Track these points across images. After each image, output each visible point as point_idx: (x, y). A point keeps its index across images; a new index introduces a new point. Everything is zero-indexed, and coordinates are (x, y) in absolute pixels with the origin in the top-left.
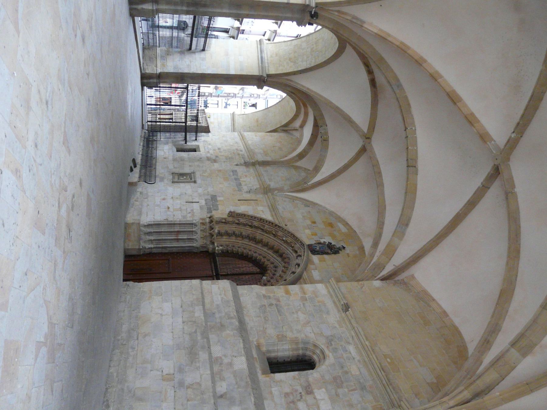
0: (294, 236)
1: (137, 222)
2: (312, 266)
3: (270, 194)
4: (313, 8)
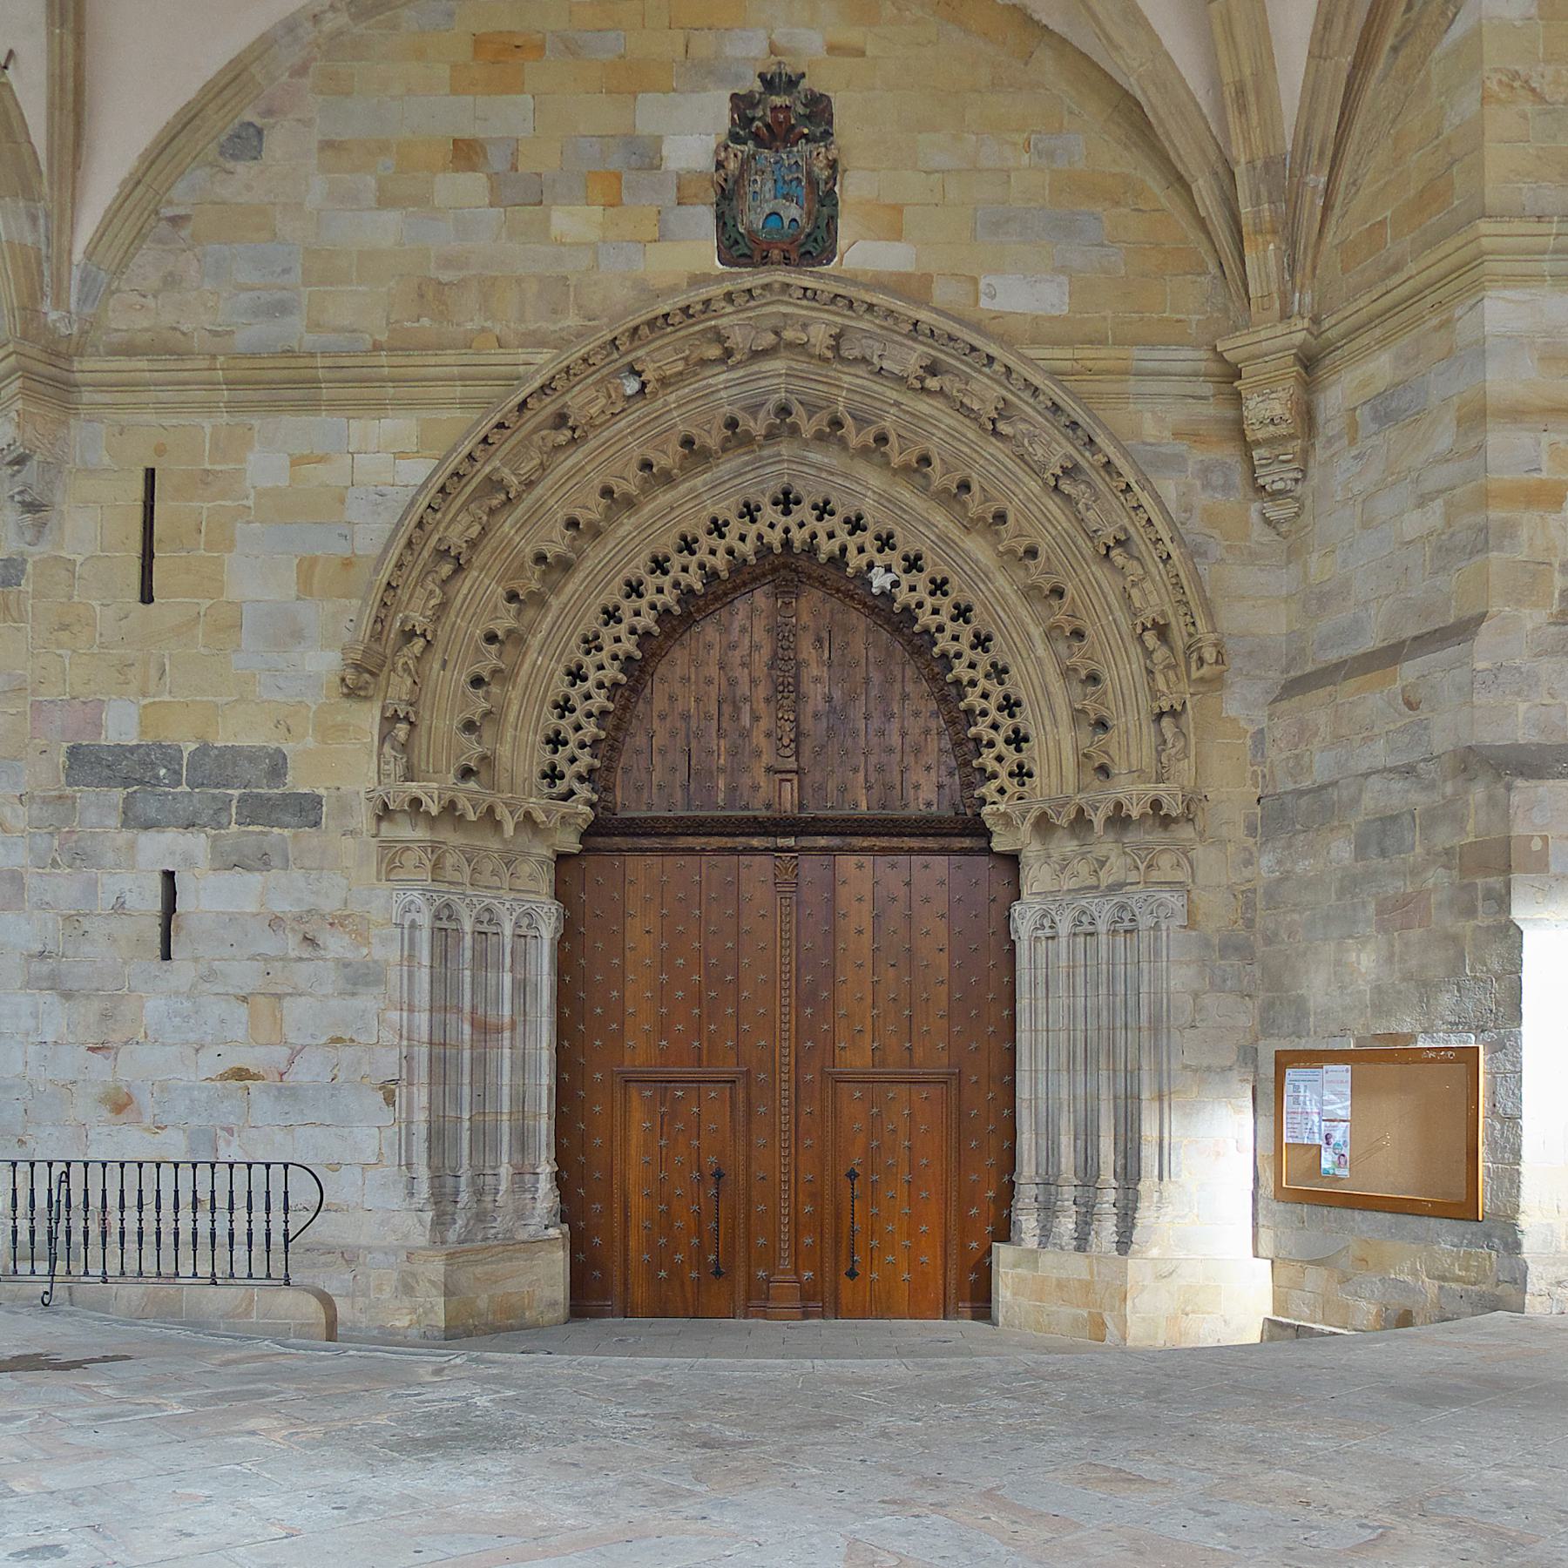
2: (943, 293)
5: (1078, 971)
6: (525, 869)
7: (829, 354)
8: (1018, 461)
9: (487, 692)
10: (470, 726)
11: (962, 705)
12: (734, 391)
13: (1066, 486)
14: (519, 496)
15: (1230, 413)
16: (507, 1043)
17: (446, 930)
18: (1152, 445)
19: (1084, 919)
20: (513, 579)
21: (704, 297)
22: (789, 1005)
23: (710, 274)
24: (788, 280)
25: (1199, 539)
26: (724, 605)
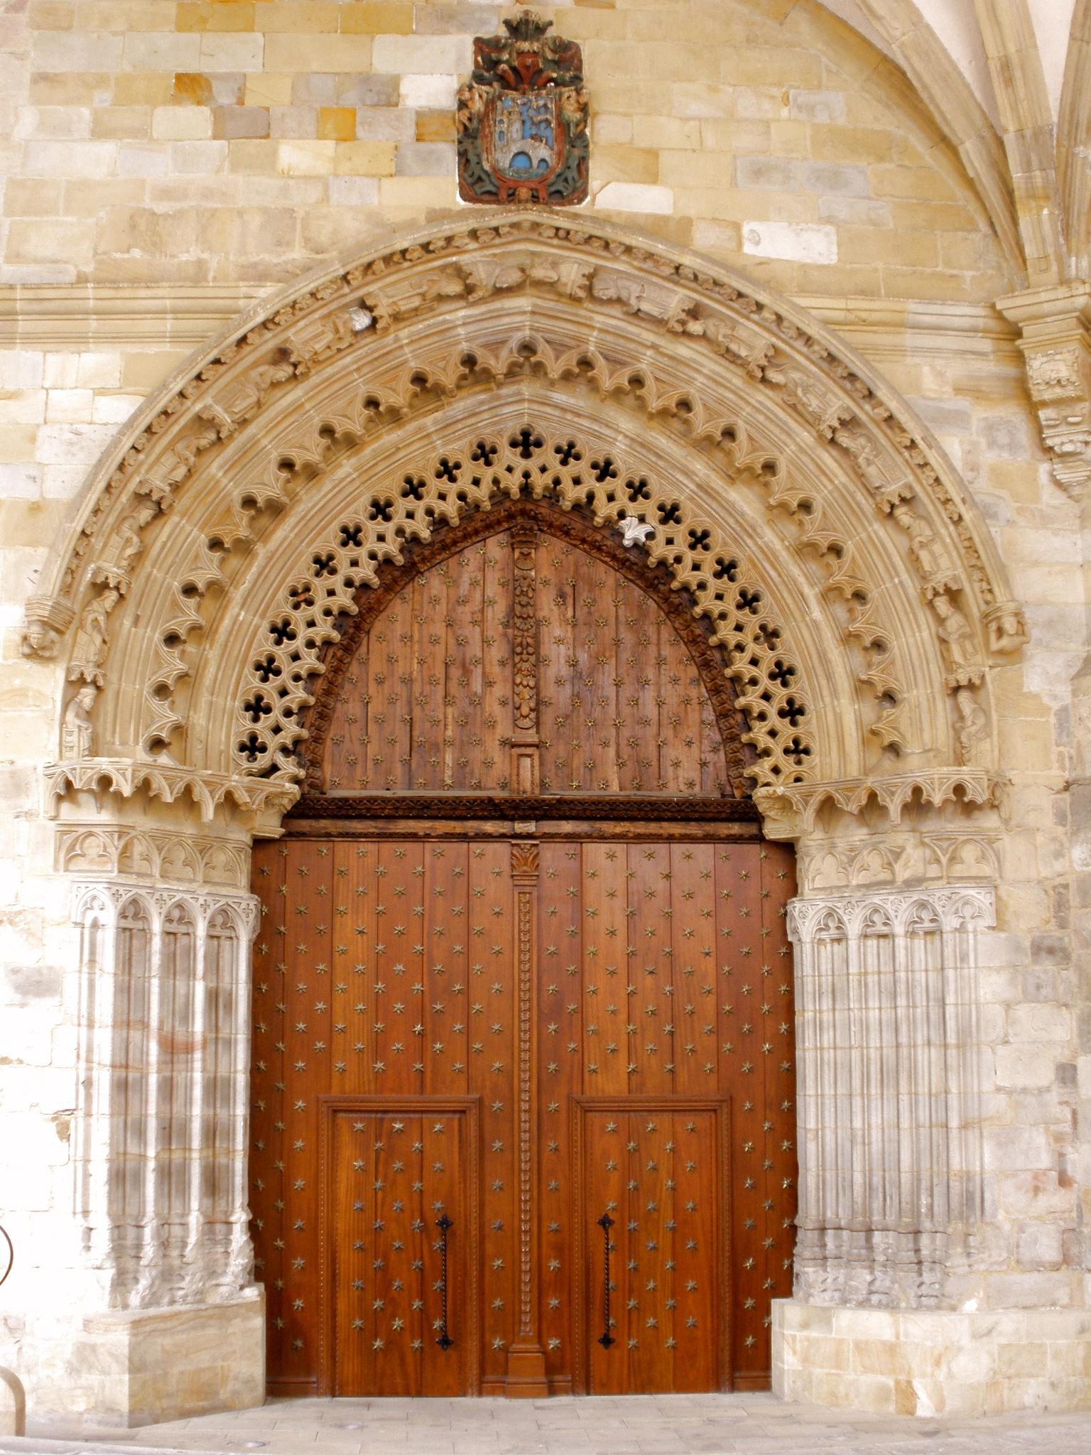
2: (705, 237)
5: (870, 978)
6: (220, 858)
7: (581, 294)
8: (789, 410)
9: (183, 652)
10: (161, 690)
11: (728, 672)
12: (471, 328)
13: (844, 438)
14: (230, 436)
15: (1010, 370)
16: (198, 1065)
17: (131, 930)
18: (930, 399)
19: (876, 918)
20: (218, 525)
21: (448, 233)
22: (529, 1020)
23: (450, 210)
24: (538, 220)
25: (988, 500)
26: (452, 555)
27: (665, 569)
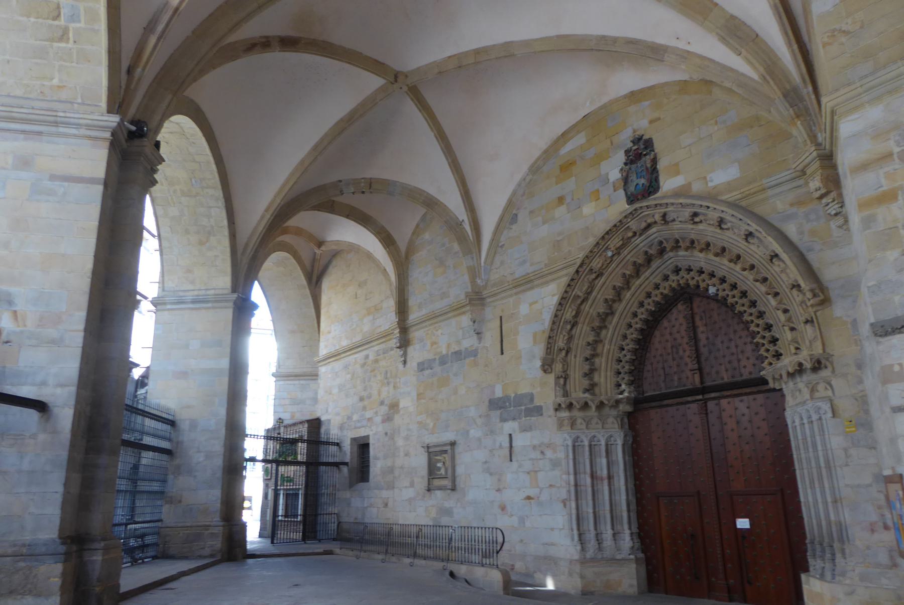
0: (607, 233)
1: (577, 568)
2: (696, 187)
3: (485, 292)
4: (121, 124)
27: (725, 299)
